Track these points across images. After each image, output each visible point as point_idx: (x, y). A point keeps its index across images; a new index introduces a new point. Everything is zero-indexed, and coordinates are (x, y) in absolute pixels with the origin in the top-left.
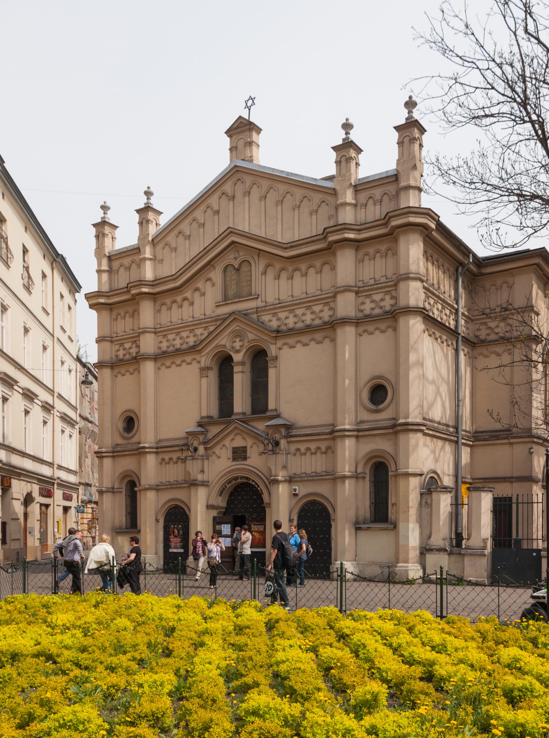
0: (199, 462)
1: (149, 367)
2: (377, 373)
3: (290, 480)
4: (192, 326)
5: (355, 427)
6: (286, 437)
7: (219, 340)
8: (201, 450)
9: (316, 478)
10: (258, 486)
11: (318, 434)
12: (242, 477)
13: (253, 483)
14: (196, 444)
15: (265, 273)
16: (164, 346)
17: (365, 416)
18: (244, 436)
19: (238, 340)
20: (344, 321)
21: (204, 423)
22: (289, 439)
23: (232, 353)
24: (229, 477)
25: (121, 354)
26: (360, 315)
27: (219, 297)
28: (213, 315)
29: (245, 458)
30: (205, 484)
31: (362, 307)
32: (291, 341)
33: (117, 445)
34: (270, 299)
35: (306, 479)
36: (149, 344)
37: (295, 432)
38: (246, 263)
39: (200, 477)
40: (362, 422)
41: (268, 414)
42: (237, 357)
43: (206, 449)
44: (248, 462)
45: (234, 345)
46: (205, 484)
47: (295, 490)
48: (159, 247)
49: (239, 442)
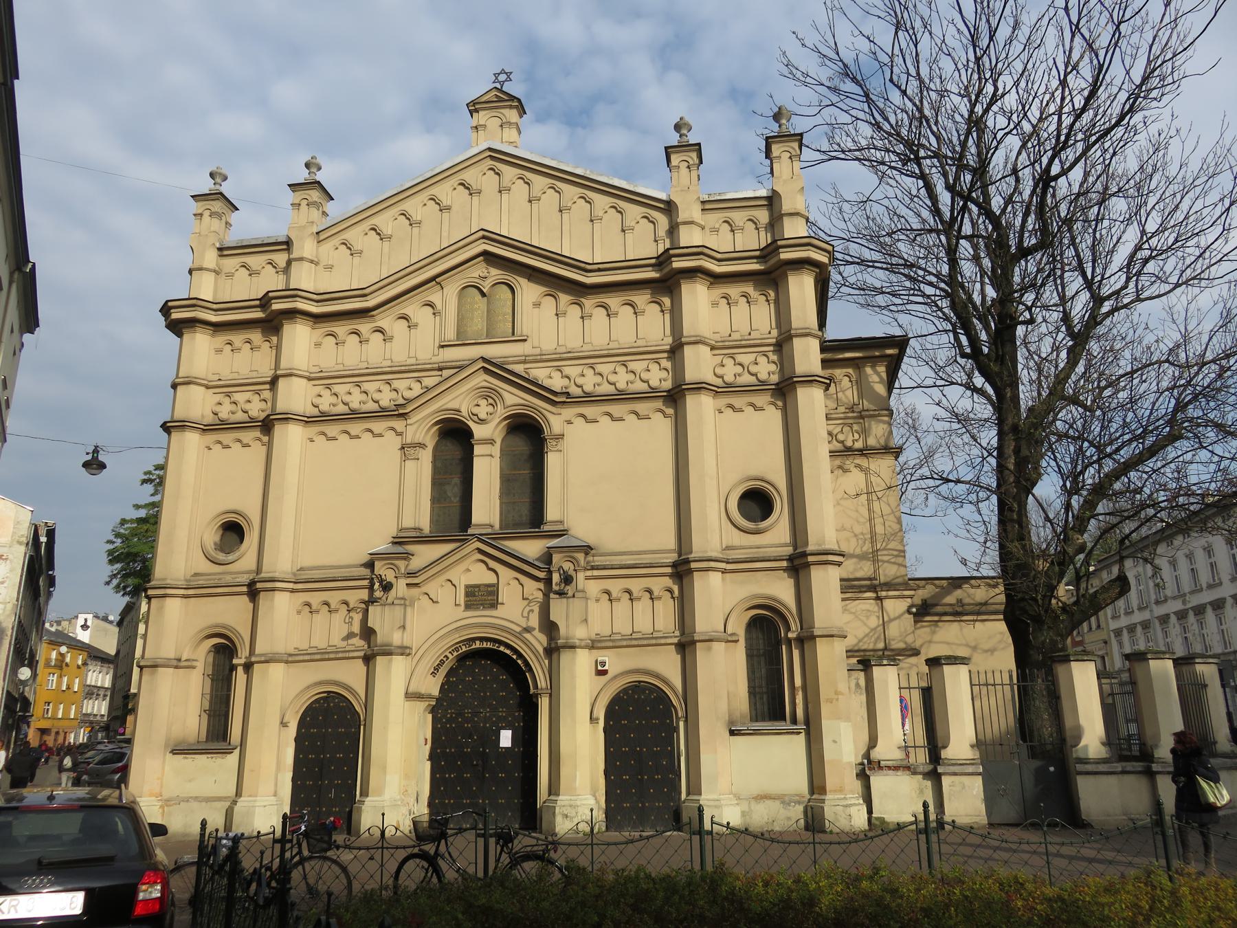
0: (398, 611)
1: (291, 437)
2: (754, 472)
3: (593, 645)
4: (389, 374)
6: (586, 569)
7: (450, 397)
8: (400, 588)
9: (645, 642)
10: (520, 656)
11: (651, 566)
12: (482, 639)
13: (508, 652)
14: (389, 576)
15: (537, 305)
16: (326, 403)
17: (738, 538)
18: (492, 564)
19: (483, 403)
20: (699, 387)
21: (404, 541)
22: (589, 573)
23: (471, 424)
24: (457, 638)
25: (224, 412)
26: (719, 382)
27: (451, 334)
28: (435, 359)
29: (494, 605)
30: (404, 651)
31: (719, 371)
32: (589, 411)
33: (196, 574)
34: (548, 345)
35: (625, 643)
36: (296, 396)
37: (599, 561)
38: (504, 287)
39: (397, 639)
40: (728, 548)
41: (546, 528)
42: (478, 431)
44: (500, 611)
45: (475, 410)
46: (404, 651)
47: (603, 664)
48: (327, 247)
49: (479, 575)
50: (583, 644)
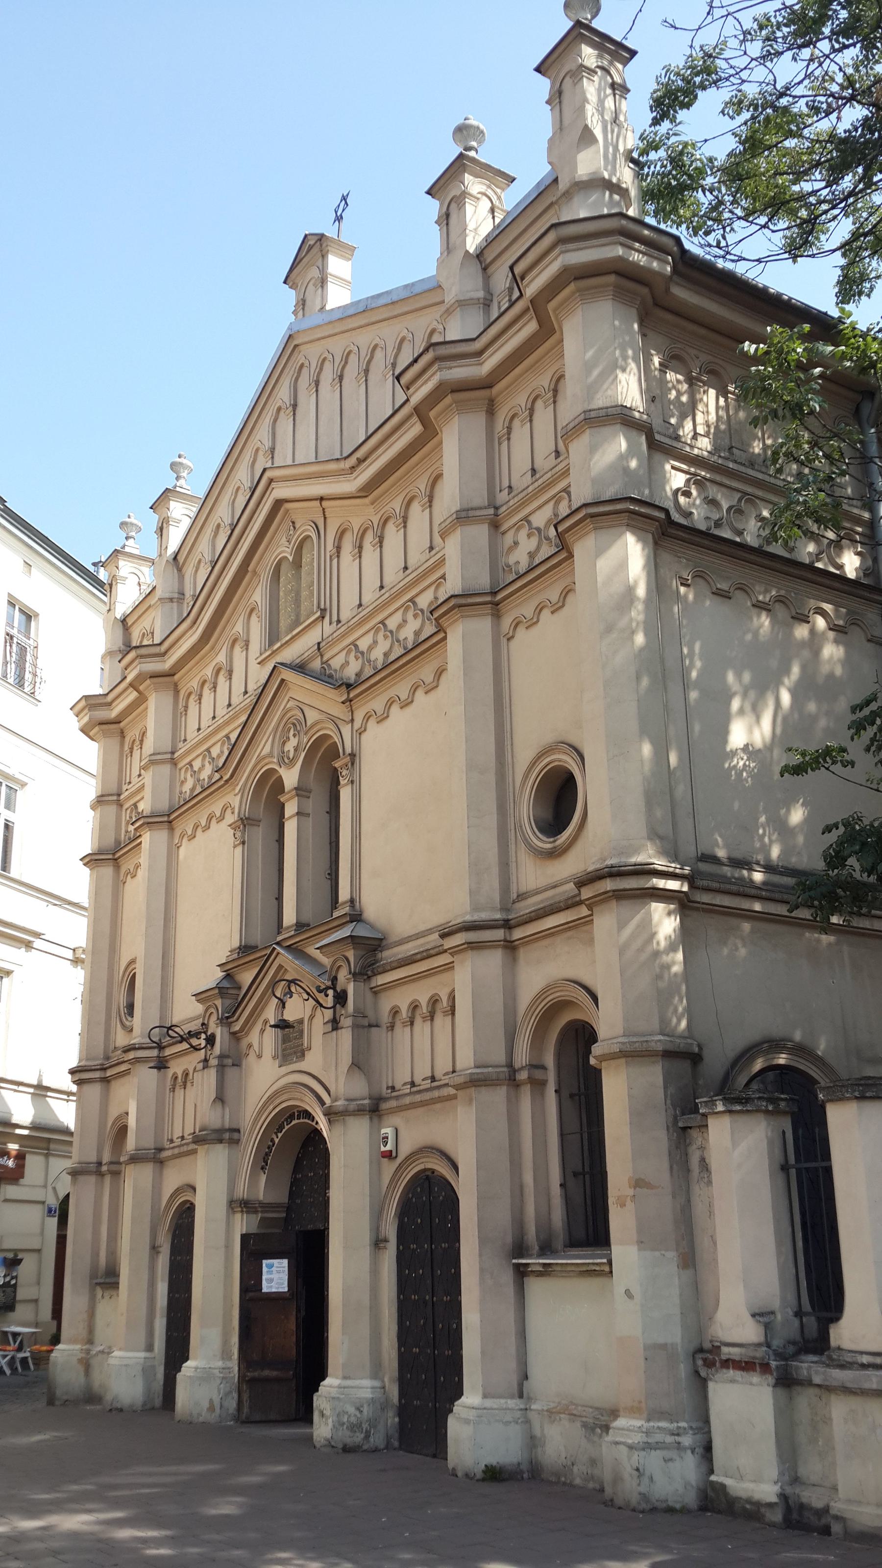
3: (375, 1109)
5: (498, 916)
30: (227, 1136)
40: (521, 897)
43: (236, 1037)
50: (353, 1106)
